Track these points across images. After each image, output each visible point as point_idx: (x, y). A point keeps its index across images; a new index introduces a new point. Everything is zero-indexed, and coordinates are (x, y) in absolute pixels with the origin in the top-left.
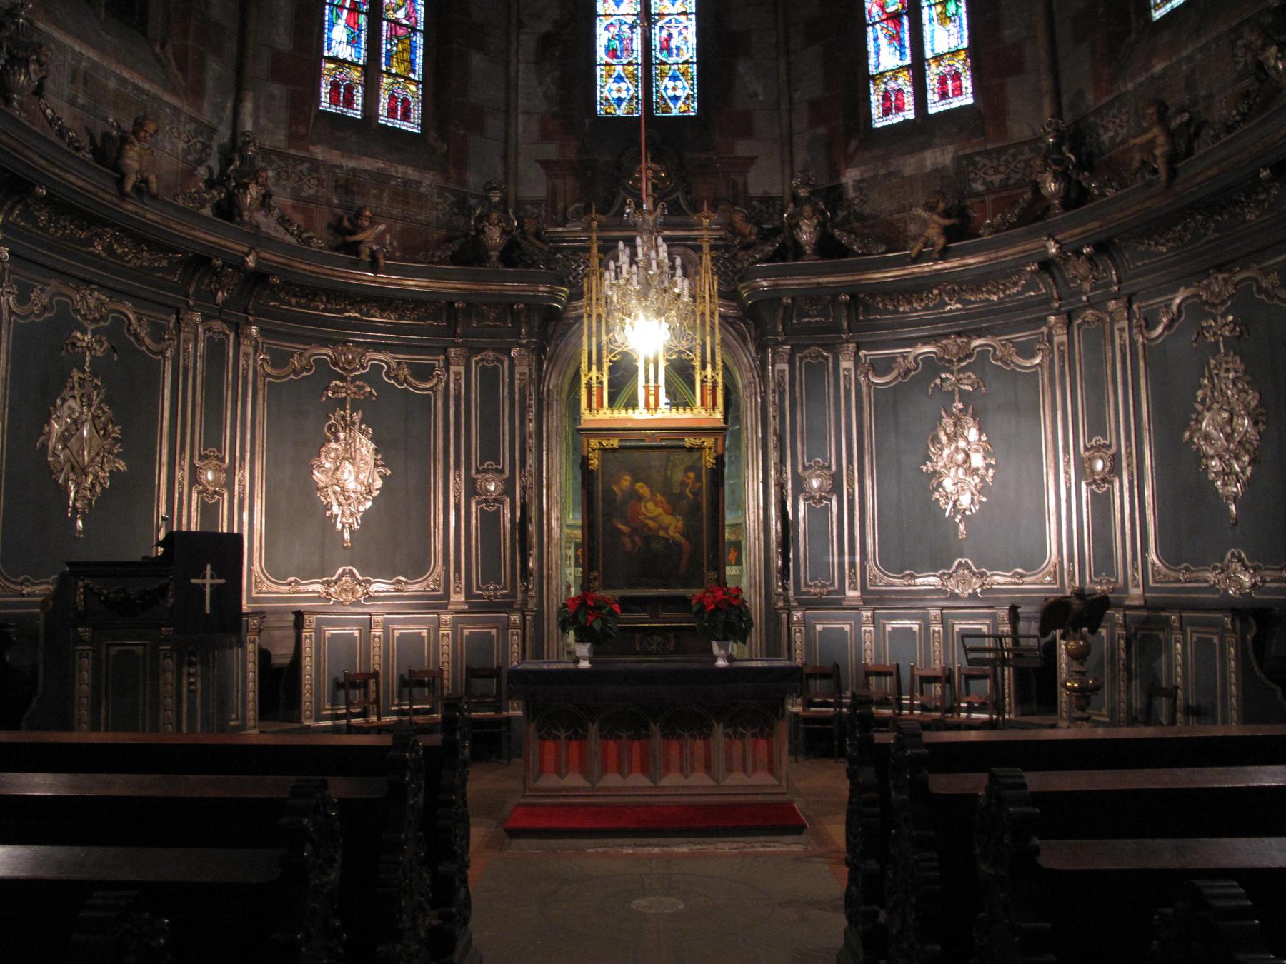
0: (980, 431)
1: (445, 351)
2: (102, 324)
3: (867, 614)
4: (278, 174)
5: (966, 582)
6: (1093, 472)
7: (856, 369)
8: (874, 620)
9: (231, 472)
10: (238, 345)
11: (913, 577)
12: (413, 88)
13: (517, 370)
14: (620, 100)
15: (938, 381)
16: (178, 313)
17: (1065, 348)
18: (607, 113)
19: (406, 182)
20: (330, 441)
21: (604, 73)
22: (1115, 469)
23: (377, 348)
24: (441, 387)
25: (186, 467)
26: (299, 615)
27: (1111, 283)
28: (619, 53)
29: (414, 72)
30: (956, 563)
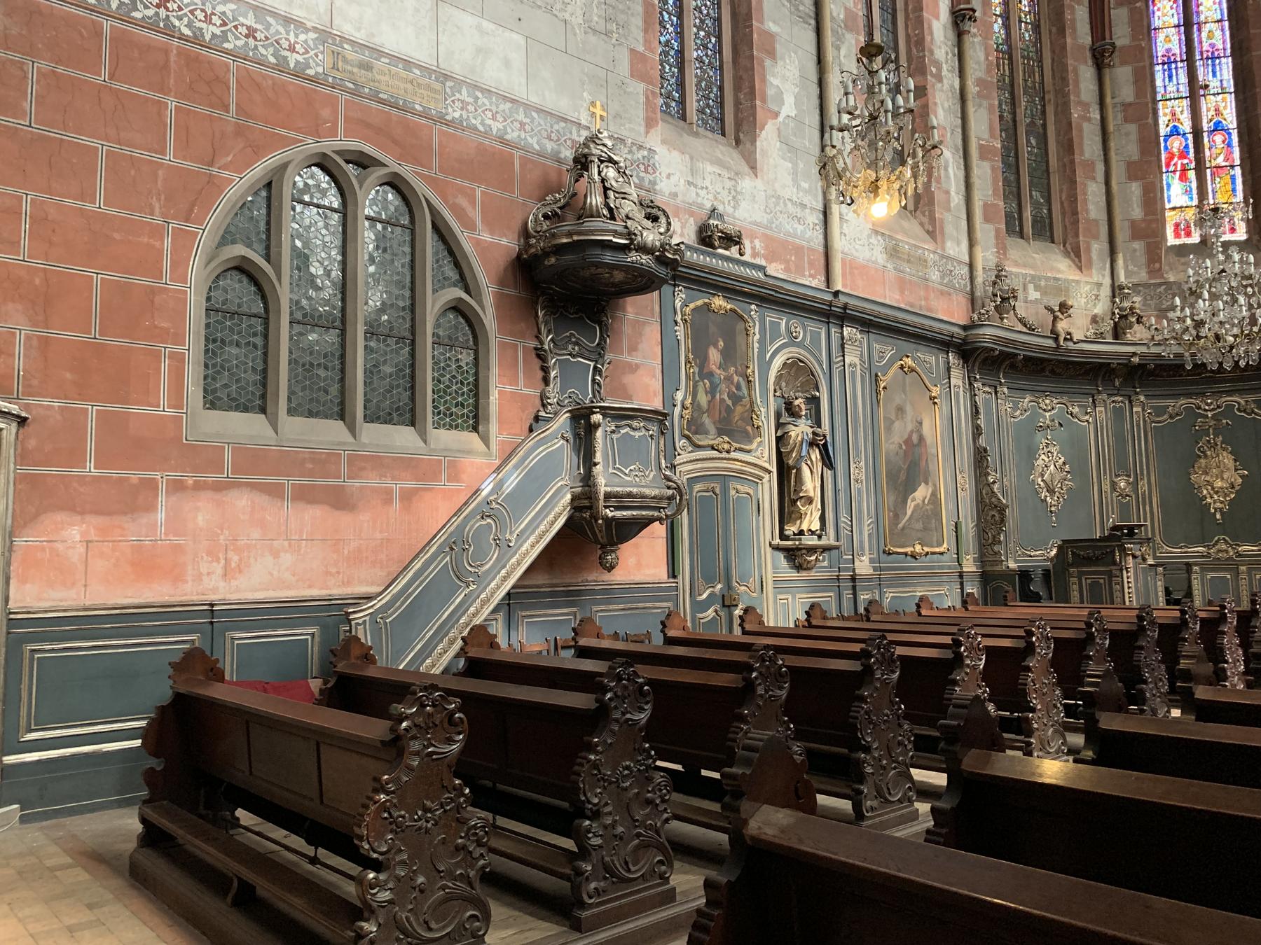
2: (1053, 412)
4: (1145, 298)
10: (1132, 407)
20: (1200, 457)
23: (1230, 393)
25: (1108, 483)
26: (1189, 565)
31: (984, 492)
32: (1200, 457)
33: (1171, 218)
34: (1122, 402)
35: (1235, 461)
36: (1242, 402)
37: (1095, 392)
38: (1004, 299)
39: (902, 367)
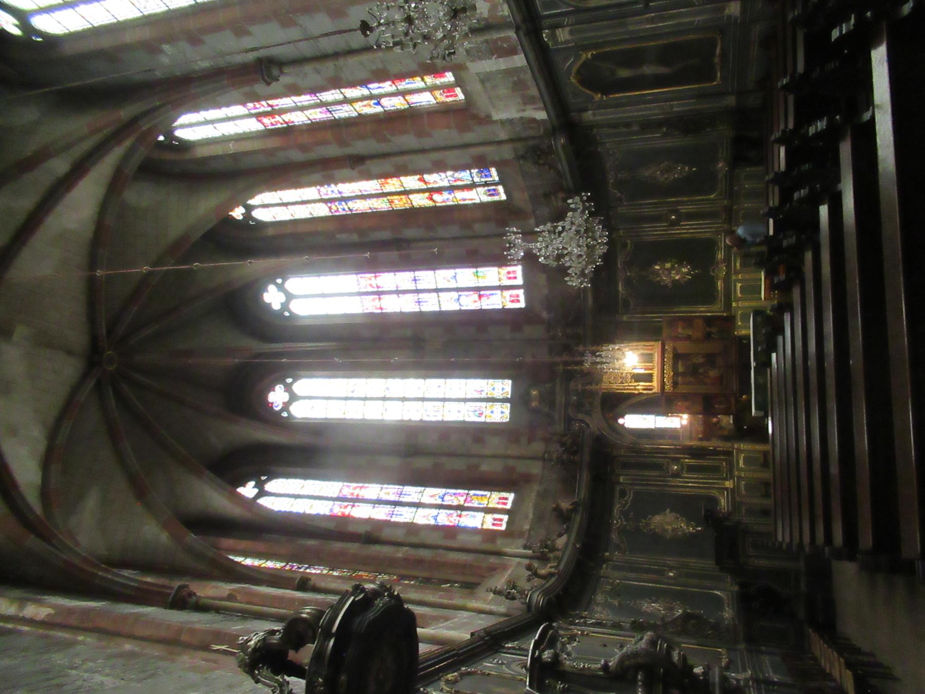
0: (656, 264)
3: (734, 304)
10: (613, 561)
12: (493, 496)
13: (622, 454)
14: (502, 412)
18: (507, 418)
21: (489, 418)
22: (676, 212)
24: (630, 487)
28: (481, 412)
29: (486, 495)
30: (712, 273)
31: (670, 630)
33: (488, 525)
36: (620, 505)
38: (514, 587)
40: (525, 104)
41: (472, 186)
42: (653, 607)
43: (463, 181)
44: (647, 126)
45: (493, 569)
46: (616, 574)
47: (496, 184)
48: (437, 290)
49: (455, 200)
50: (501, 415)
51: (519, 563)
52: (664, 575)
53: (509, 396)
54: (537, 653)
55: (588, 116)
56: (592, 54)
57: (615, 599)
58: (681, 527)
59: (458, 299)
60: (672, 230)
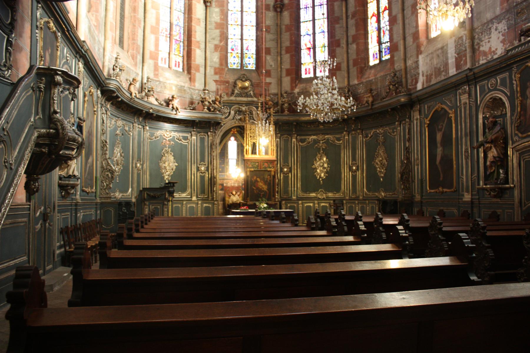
0: (327, 158)
1: (191, 132)
3: (300, 202)
5: (322, 195)
6: (353, 169)
7: (297, 140)
8: (302, 204)
9: (142, 165)
10: (144, 131)
11: (309, 194)
13: (210, 138)
15: (317, 145)
16: (133, 124)
17: (348, 140)
19: (181, 86)
20: (163, 156)
22: (357, 169)
27: (358, 126)
30: (320, 190)
31: (104, 162)
32: (163, 156)
34: (141, 128)
35: (174, 159)
37: (133, 122)
39: (90, 92)
40: (427, 76)
41: (380, 43)
42: (118, 153)
43: (383, 37)
44: (408, 150)
45: (134, 57)
46: (136, 133)
47: (380, 59)
48: (314, 20)
49: (372, 31)
50: (232, 62)
51: (138, 74)
52: (138, 161)
53: (245, 68)
54: (60, 73)
55: (416, 115)
56: (451, 117)
57: (120, 132)
58: (167, 171)
59: (308, 35)
60: (347, 167)
